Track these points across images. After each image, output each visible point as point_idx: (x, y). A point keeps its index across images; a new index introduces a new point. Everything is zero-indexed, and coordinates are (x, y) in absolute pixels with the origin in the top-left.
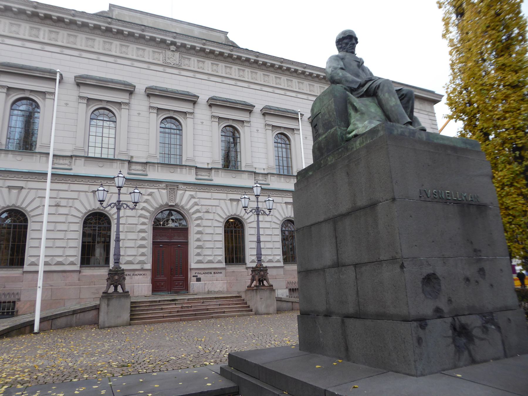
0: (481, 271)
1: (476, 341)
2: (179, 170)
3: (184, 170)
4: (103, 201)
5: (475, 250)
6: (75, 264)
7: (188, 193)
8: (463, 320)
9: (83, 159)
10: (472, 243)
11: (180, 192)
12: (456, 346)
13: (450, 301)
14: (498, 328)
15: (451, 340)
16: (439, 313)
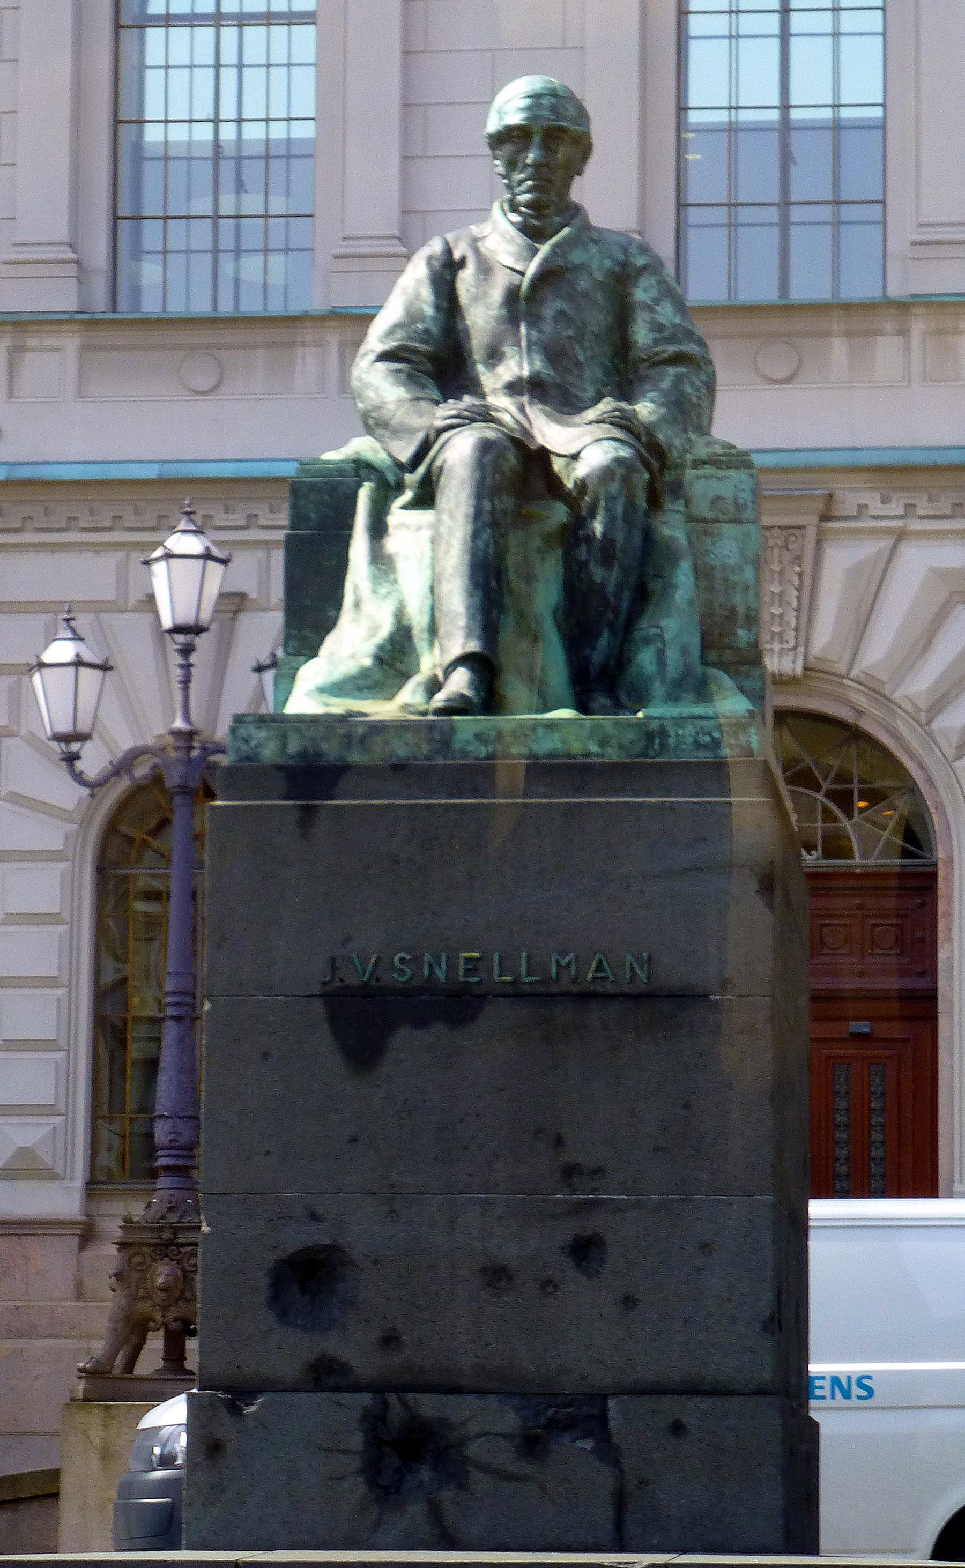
0: (585, 1250)
1: (479, 1481)
2: (839, 348)
3: (887, 349)
4: (83, 737)
5: (570, 1172)
6: (48, 1175)
7: (918, 563)
8: (428, 1405)
9: (71, 343)
10: (559, 1141)
11: (841, 561)
12: (372, 1482)
13: (390, 1341)
14: (607, 1450)
15: (354, 1463)
16: (325, 1375)
